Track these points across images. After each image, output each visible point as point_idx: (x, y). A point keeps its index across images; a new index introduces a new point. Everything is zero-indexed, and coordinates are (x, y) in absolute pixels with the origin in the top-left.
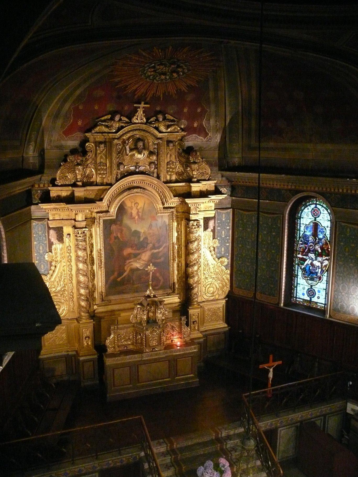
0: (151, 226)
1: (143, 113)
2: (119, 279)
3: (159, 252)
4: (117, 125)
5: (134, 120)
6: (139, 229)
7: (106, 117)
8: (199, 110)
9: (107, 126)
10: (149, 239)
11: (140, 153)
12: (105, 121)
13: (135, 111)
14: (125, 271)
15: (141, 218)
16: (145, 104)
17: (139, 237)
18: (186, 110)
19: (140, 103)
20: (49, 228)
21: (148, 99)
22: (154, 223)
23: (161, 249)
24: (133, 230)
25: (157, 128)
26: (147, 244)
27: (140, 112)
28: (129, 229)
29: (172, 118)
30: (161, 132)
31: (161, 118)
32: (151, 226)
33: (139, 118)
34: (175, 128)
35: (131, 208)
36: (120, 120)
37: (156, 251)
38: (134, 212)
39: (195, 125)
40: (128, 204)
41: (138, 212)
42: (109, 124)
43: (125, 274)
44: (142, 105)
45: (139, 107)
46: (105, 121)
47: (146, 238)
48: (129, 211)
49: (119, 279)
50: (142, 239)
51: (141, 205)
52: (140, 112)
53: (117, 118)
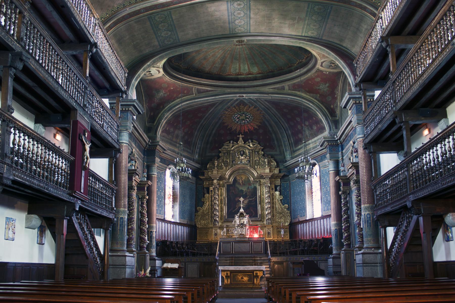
0: (248, 188)
1: (242, 139)
2: (233, 211)
3: (252, 200)
4: (231, 145)
5: (239, 142)
6: (243, 189)
7: (227, 142)
8: (268, 137)
9: (228, 146)
10: (248, 194)
11: (242, 156)
12: (227, 144)
13: (238, 139)
14: (236, 208)
15: (244, 185)
16: (242, 135)
17: (243, 193)
18: (261, 138)
19: (240, 135)
20: (204, 188)
21: (243, 133)
22: (250, 187)
23: (253, 199)
24: (240, 189)
25: (249, 146)
26: (247, 196)
27: (241, 139)
28: (238, 189)
29: (255, 141)
30: (250, 147)
31: (250, 141)
32: (248, 188)
33: (241, 142)
34: (257, 145)
35: (239, 180)
36: (233, 143)
37: (251, 199)
38: (241, 182)
39: (268, 144)
40: (238, 178)
41: (242, 182)
42: (229, 145)
43: (236, 209)
44: (241, 136)
45: (240, 137)
46: (227, 144)
47: (246, 193)
48: (238, 181)
49: (233, 211)
50: (244, 193)
51: (244, 179)
52: (241, 139)
53: (232, 142)
